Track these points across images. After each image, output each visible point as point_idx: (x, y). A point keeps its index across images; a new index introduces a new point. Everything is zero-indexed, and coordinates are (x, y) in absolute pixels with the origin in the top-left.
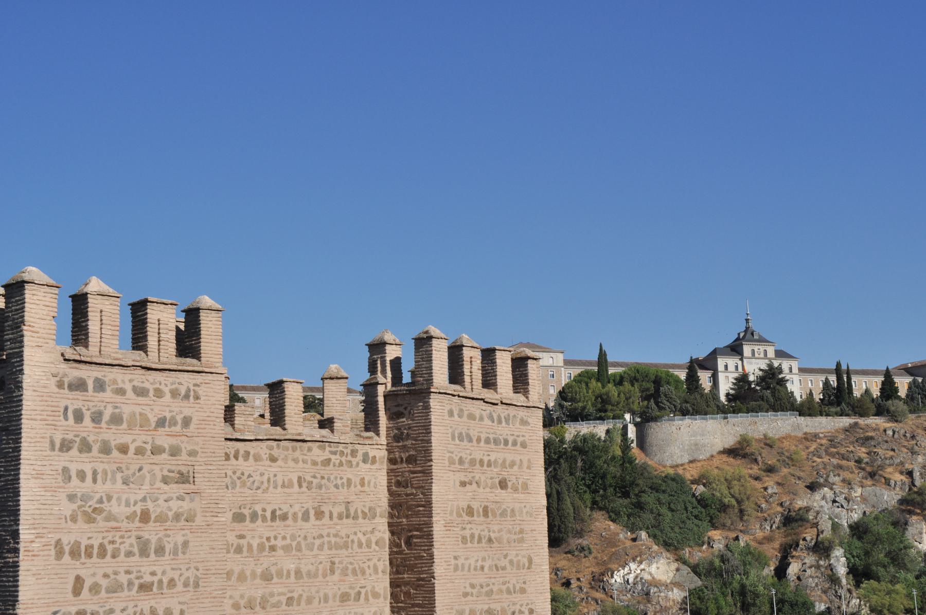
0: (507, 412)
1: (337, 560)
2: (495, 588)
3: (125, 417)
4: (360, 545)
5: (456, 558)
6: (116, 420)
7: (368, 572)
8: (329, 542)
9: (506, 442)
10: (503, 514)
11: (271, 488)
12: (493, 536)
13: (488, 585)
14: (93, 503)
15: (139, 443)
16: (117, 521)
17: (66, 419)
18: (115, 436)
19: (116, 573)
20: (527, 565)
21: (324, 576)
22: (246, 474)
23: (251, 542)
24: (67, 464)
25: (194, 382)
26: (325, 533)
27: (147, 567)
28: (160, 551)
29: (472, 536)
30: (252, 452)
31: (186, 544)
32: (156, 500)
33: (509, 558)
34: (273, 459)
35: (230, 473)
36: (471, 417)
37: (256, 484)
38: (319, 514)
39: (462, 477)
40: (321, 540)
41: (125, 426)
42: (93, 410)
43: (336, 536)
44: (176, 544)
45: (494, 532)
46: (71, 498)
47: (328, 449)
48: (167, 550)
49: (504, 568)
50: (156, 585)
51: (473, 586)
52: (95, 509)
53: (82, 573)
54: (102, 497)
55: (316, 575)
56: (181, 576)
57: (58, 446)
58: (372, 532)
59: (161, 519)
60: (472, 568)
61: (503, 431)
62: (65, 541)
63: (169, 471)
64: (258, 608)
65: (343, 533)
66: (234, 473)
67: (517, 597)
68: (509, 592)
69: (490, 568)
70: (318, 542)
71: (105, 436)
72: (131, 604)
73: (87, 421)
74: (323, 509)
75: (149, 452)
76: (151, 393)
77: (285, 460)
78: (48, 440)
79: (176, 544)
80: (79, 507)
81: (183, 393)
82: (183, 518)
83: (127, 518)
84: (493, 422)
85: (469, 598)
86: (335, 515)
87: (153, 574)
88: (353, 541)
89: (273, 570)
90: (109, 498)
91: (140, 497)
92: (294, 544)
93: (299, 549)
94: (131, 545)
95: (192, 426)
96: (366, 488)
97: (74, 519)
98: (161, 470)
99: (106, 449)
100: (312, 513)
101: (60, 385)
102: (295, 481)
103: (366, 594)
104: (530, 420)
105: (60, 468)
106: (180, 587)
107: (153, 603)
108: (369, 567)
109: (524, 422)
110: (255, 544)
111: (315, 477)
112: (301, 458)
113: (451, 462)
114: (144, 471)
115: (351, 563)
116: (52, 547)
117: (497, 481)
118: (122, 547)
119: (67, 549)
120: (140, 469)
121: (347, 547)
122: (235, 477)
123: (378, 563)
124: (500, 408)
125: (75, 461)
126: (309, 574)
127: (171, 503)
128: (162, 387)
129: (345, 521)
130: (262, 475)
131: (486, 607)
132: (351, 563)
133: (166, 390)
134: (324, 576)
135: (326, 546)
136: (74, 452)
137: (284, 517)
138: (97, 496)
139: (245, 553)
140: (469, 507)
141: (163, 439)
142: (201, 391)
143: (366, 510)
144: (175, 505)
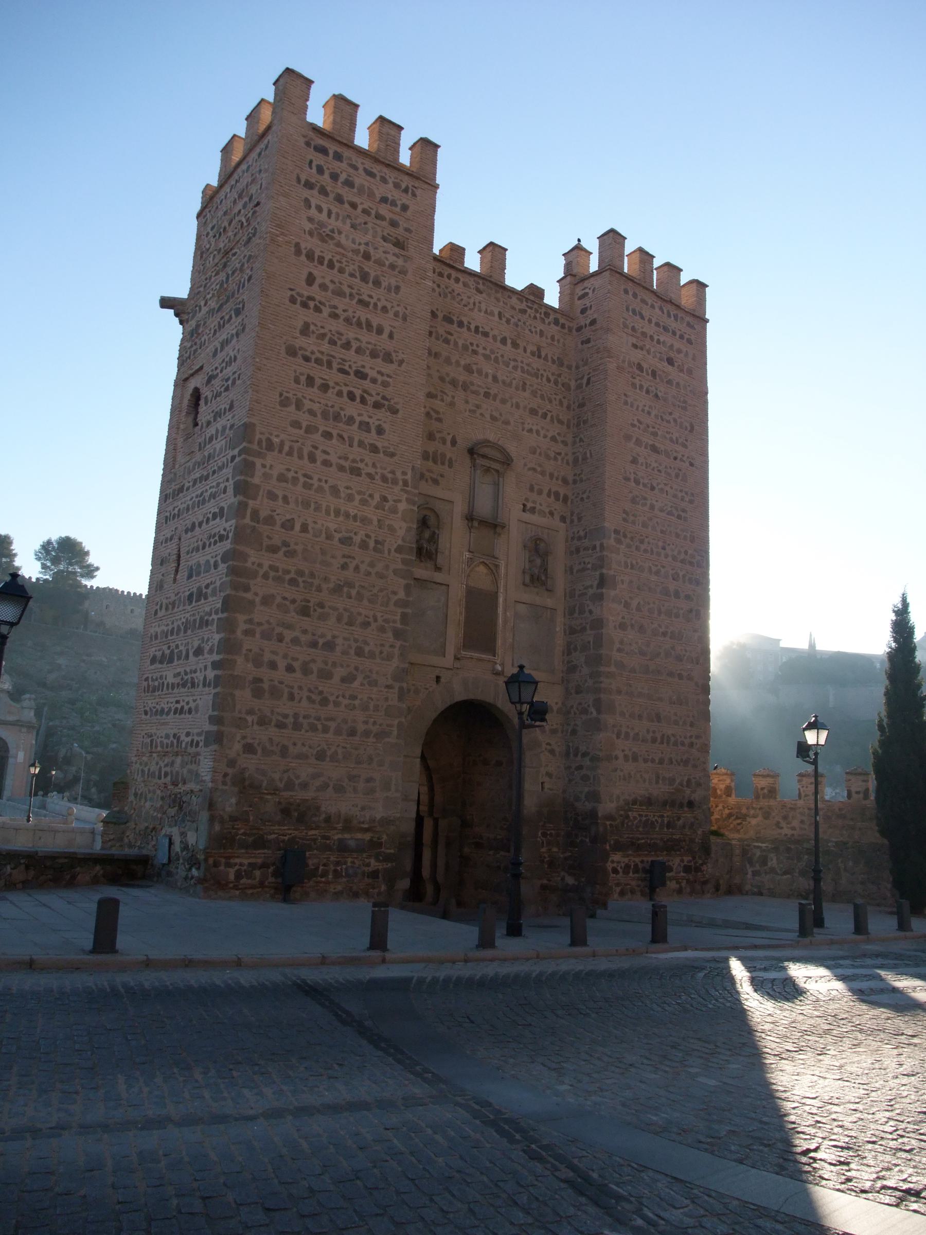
0: (675, 312)
1: (528, 383)
2: (660, 433)
3: (356, 185)
4: (549, 380)
5: (625, 395)
6: (349, 184)
7: (554, 402)
8: (522, 367)
9: (674, 333)
10: (669, 382)
11: (476, 310)
12: (660, 394)
14: (327, 230)
15: (365, 206)
16: (345, 249)
17: (311, 168)
18: (345, 192)
19: (341, 283)
20: (689, 428)
22: (456, 292)
23: (457, 340)
24: (309, 197)
25: (413, 184)
26: (519, 359)
27: (366, 290)
28: (377, 283)
30: (462, 279)
31: (398, 288)
32: (376, 248)
33: (673, 416)
34: (480, 291)
35: (442, 286)
36: (644, 301)
37: (463, 302)
38: (515, 345)
39: (634, 340)
40: (516, 363)
41: (355, 190)
42: (332, 171)
43: (528, 365)
44: (389, 284)
45: (660, 391)
46: (310, 220)
47: (525, 303)
48: (383, 287)
49: (668, 422)
50: (372, 305)
52: (327, 235)
53: (315, 273)
54: (333, 229)
55: (510, 385)
56: (392, 307)
57: (303, 182)
58: (559, 375)
59: (379, 263)
60: (640, 409)
61: (672, 324)
62: (303, 246)
63: (388, 234)
64: (460, 388)
65: (535, 366)
66: (447, 288)
67: (679, 448)
68: (671, 440)
69: (656, 416)
70: (512, 364)
71: (340, 191)
72: (351, 310)
73: (326, 176)
74: (518, 342)
75: (373, 216)
76: (378, 178)
77: (489, 295)
78: (296, 176)
79: (389, 284)
80: (316, 229)
81: (403, 186)
82: (397, 270)
83: (352, 251)
84: (663, 313)
85: (636, 429)
86: (529, 351)
87: (371, 297)
88: (542, 375)
89: (474, 367)
90: (340, 233)
91: (362, 242)
92: (493, 356)
93: (496, 360)
94: (354, 270)
95: (409, 213)
96: (556, 343)
97: (311, 234)
98: (383, 231)
99: (339, 199)
100: (509, 341)
101: (308, 144)
102: (496, 313)
103: (552, 417)
104: (696, 326)
105: (303, 199)
107: (369, 316)
108: (555, 399)
109: (689, 324)
111: (513, 317)
112: (502, 299)
113: (625, 326)
114: (370, 225)
115: (540, 390)
116: (293, 245)
117: (665, 357)
118: (347, 268)
119: (304, 252)
120: (365, 223)
121: (537, 378)
122: (447, 291)
123: (563, 400)
124: (669, 306)
125: (315, 198)
126: (504, 382)
127: (388, 256)
128: (387, 177)
129: (536, 358)
130: (469, 298)
131: (652, 443)
132: (540, 390)
133: (390, 181)
134: (517, 388)
135: (519, 369)
136: (315, 192)
137: (486, 334)
138: (330, 227)
139: (452, 346)
140: (639, 364)
141: (384, 210)
142: (418, 192)
143: (555, 358)
144: (392, 259)
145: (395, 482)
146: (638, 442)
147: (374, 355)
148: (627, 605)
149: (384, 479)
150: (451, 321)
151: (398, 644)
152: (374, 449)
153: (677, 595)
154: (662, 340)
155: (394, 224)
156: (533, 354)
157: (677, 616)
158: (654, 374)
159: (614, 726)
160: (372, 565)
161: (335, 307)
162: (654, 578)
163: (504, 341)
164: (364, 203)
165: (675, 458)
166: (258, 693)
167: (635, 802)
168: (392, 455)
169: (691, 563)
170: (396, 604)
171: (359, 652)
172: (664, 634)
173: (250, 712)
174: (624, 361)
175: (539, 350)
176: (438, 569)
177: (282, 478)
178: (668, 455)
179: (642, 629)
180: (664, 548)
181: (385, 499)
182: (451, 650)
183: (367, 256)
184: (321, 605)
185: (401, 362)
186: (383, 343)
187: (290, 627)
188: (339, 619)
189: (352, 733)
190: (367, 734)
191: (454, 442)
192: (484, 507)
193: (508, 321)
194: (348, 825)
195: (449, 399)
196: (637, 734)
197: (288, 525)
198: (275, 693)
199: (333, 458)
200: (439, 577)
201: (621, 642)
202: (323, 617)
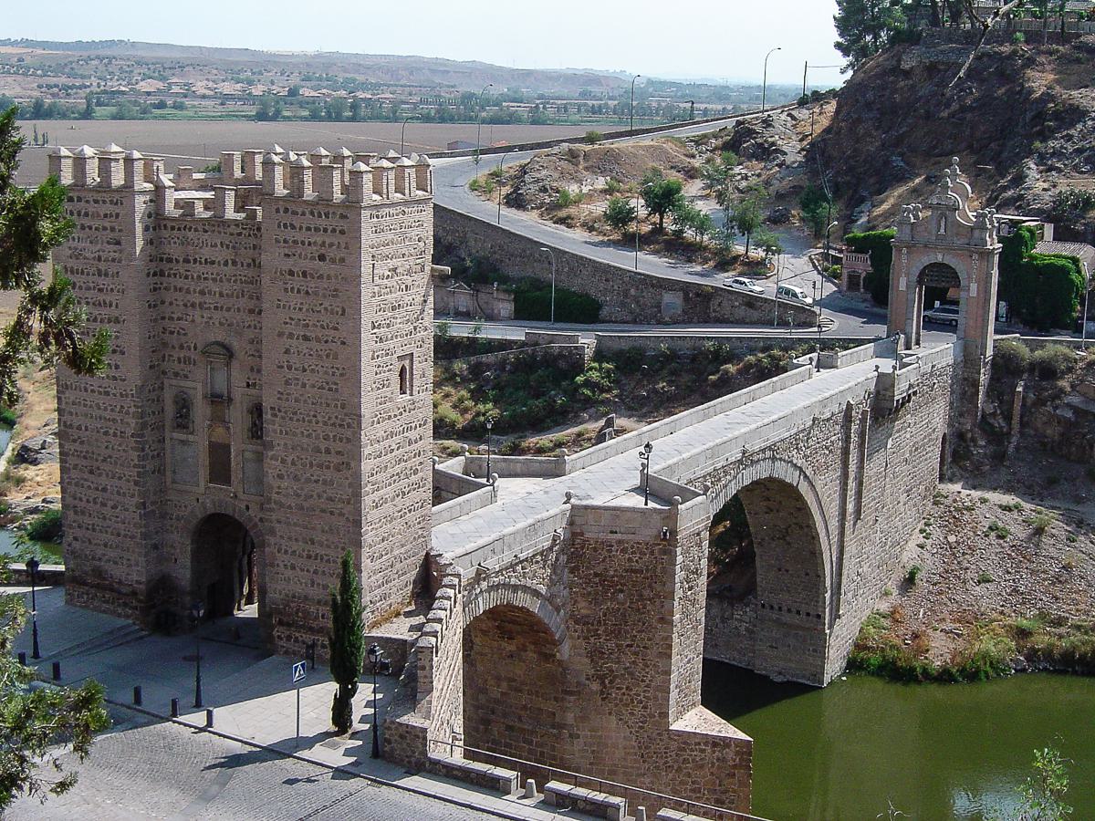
1: (246, 290)
2: (311, 323)
6: (86, 215)
10: (321, 277)
13: (305, 320)
18: (87, 221)
20: (340, 313)
21: (238, 297)
28: (106, 275)
29: (292, 288)
31: (118, 273)
36: (295, 213)
43: (245, 276)
51: (292, 319)
69: (307, 310)
70: (233, 279)
86: (245, 264)
87: (104, 284)
93: (221, 281)
100: (230, 262)
102: (219, 244)
106: (115, 292)
110: (195, 276)
113: (277, 241)
121: (253, 284)
126: (227, 295)
131: (302, 333)
134: (238, 297)
140: (290, 270)
145: (127, 396)
146: (291, 336)
147: (109, 321)
148: (283, 461)
149: (121, 395)
150: (188, 262)
151: (137, 488)
152: (115, 378)
153: (328, 451)
154: (312, 240)
155: (113, 229)
156: (249, 265)
157: (328, 467)
158: (304, 274)
159: (275, 544)
160: (120, 445)
161: (87, 298)
162: (305, 440)
163: (226, 264)
164: (96, 223)
165: (326, 342)
166: (76, 512)
167: (294, 596)
168: (124, 380)
169: (341, 425)
170: (134, 467)
171: (118, 493)
172: (317, 481)
173: (74, 521)
174: (276, 273)
175: (254, 260)
176: (192, 433)
177: (74, 403)
178: (318, 340)
179: (296, 478)
180: (315, 416)
181: (122, 407)
182: (202, 484)
183: (99, 259)
184: (98, 469)
185: (124, 321)
186: (114, 312)
187: (86, 480)
188: (107, 475)
189: (119, 535)
190: (125, 536)
191: (195, 348)
192: (221, 386)
193: (228, 247)
194: (120, 582)
195: (190, 318)
196: (295, 551)
197: (79, 428)
198: (83, 513)
199: (96, 389)
200: (191, 438)
201: (279, 487)
202: (100, 475)
